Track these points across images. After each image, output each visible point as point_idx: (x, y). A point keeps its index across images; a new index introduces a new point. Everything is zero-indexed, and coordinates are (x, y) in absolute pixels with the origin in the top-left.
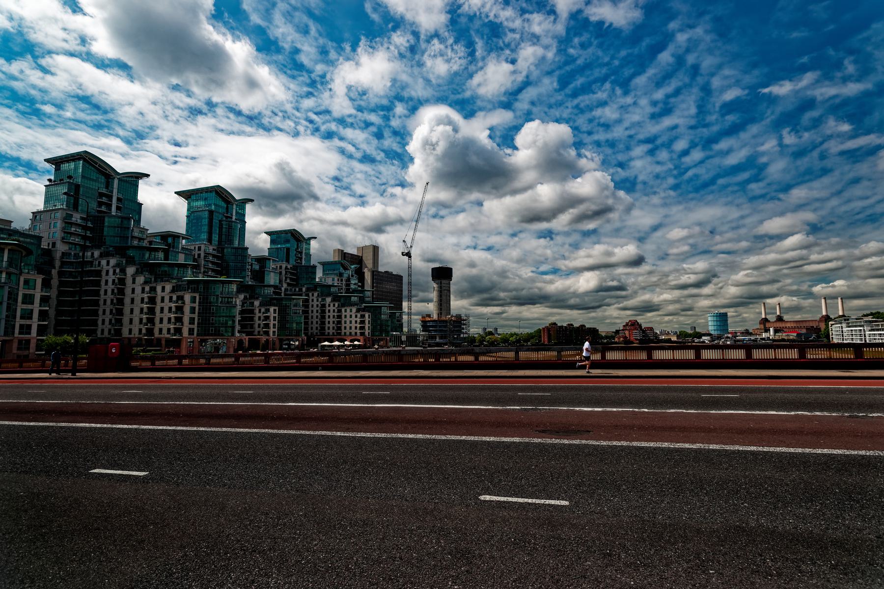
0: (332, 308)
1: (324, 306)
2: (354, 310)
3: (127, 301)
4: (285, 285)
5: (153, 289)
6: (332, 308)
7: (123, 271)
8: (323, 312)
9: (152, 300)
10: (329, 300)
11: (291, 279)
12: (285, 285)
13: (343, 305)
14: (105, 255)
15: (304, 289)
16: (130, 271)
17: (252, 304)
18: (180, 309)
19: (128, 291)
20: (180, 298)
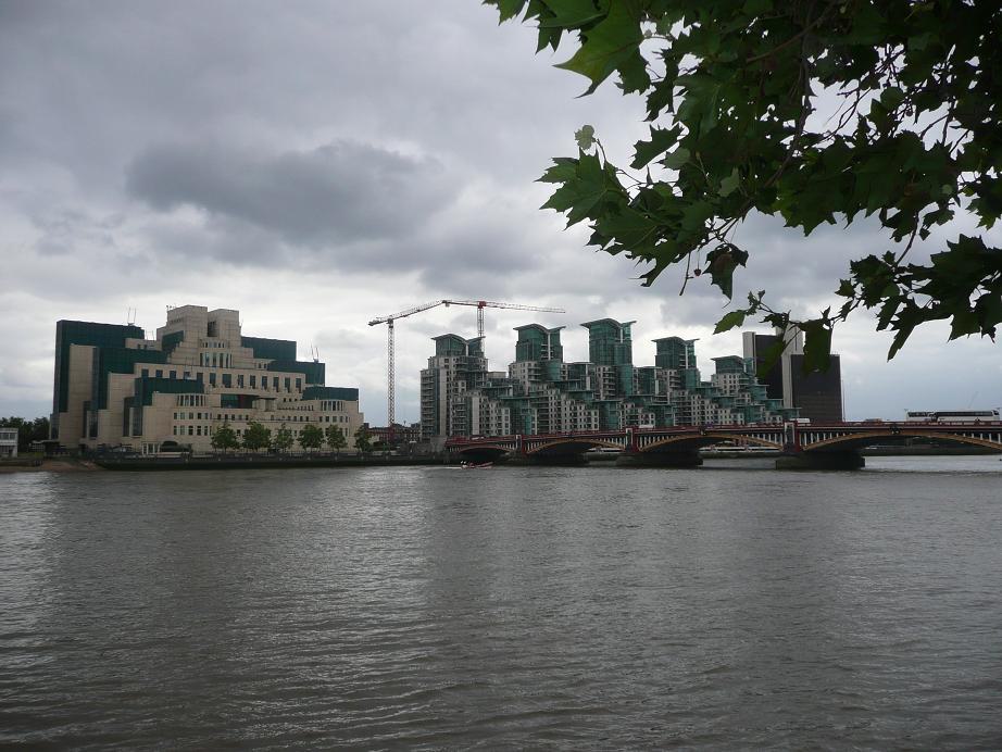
0: (710, 410)
1: (703, 408)
2: (728, 411)
3: (563, 415)
4: (670, 390)
5: (576, 409)
6: (710, 410)
7: (559, 397)
8: (703, 413)
9: (575, 414)
10: (707, 402)
11: (676, 384)
12: (670, 390)
13: (720, 406)
14: (550, 387)
15: (687, 393)
16: (564, 397)
17: (636, 411)
18: (589, 420)
19: (563, 409)
20: (589, 413)
